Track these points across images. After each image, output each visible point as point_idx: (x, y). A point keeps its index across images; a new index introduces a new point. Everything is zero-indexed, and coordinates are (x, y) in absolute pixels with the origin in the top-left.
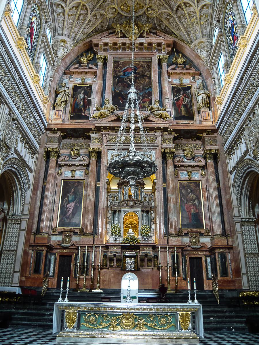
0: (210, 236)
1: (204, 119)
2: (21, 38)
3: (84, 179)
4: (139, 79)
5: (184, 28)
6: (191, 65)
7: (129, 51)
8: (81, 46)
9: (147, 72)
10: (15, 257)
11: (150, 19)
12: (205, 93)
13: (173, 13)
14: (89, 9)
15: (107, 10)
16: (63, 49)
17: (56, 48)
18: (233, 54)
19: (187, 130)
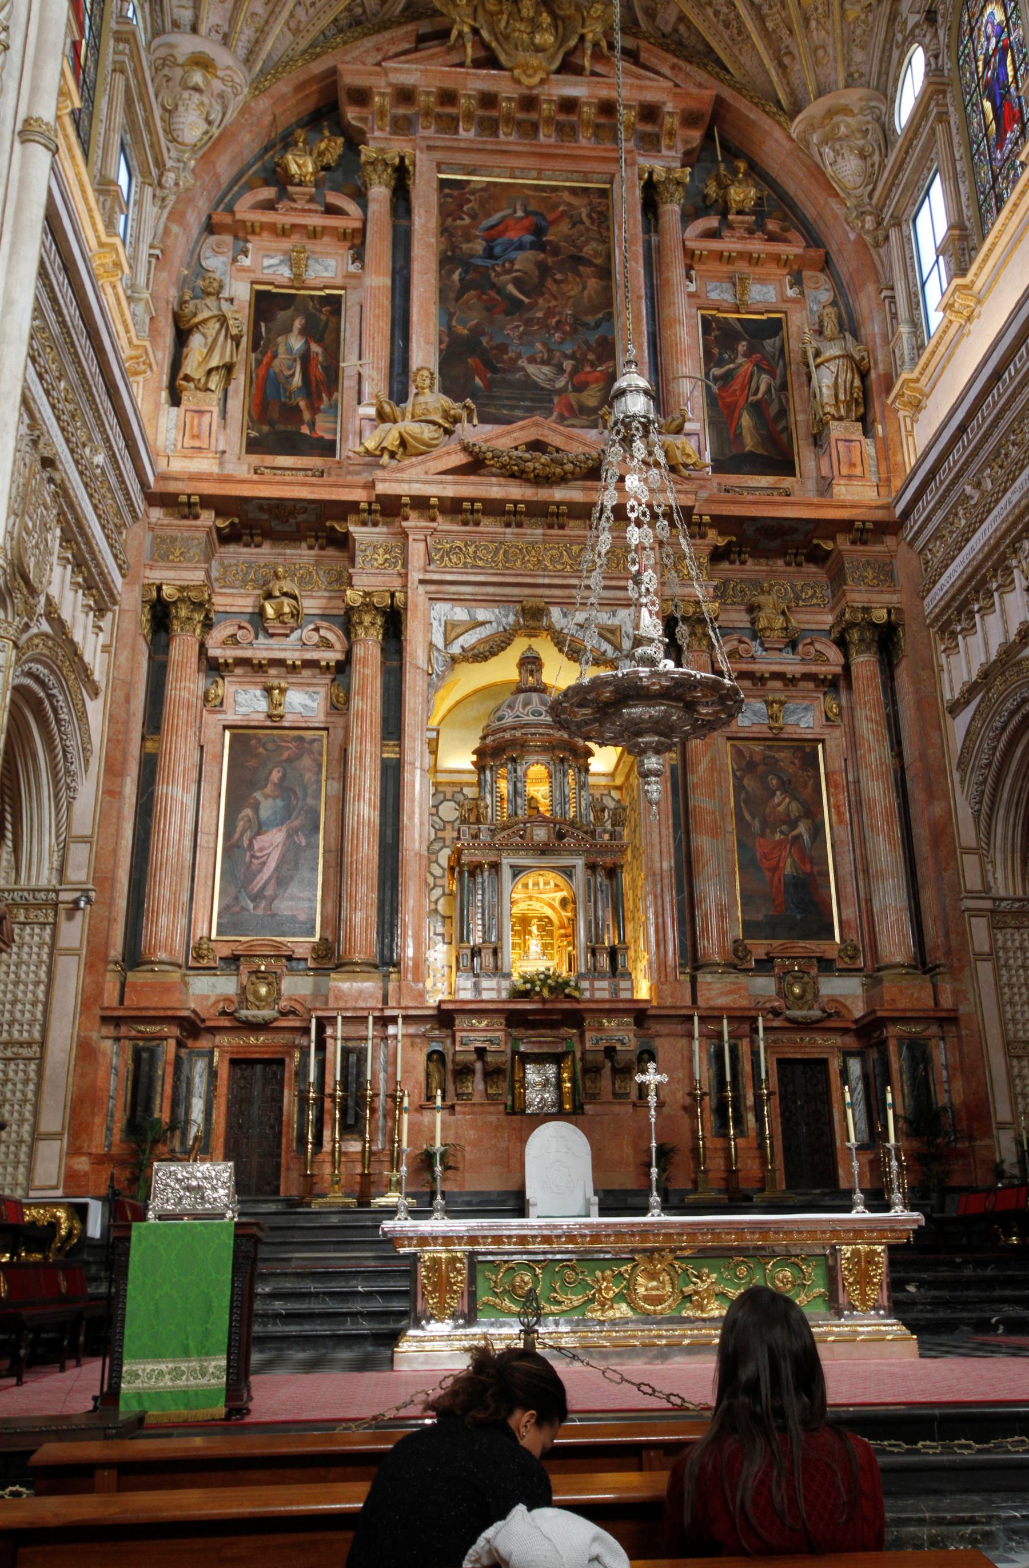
0: (860, 970)
1: (844, 471)
3: (327, 729)
4: (558, 276)
5: (766, 34)
6: (786, 215)
7: (512, 138)
8: (283, 97)
9: (594, 245)
10: (40, 1072)
12: (849, 357)
18: (993, 188)
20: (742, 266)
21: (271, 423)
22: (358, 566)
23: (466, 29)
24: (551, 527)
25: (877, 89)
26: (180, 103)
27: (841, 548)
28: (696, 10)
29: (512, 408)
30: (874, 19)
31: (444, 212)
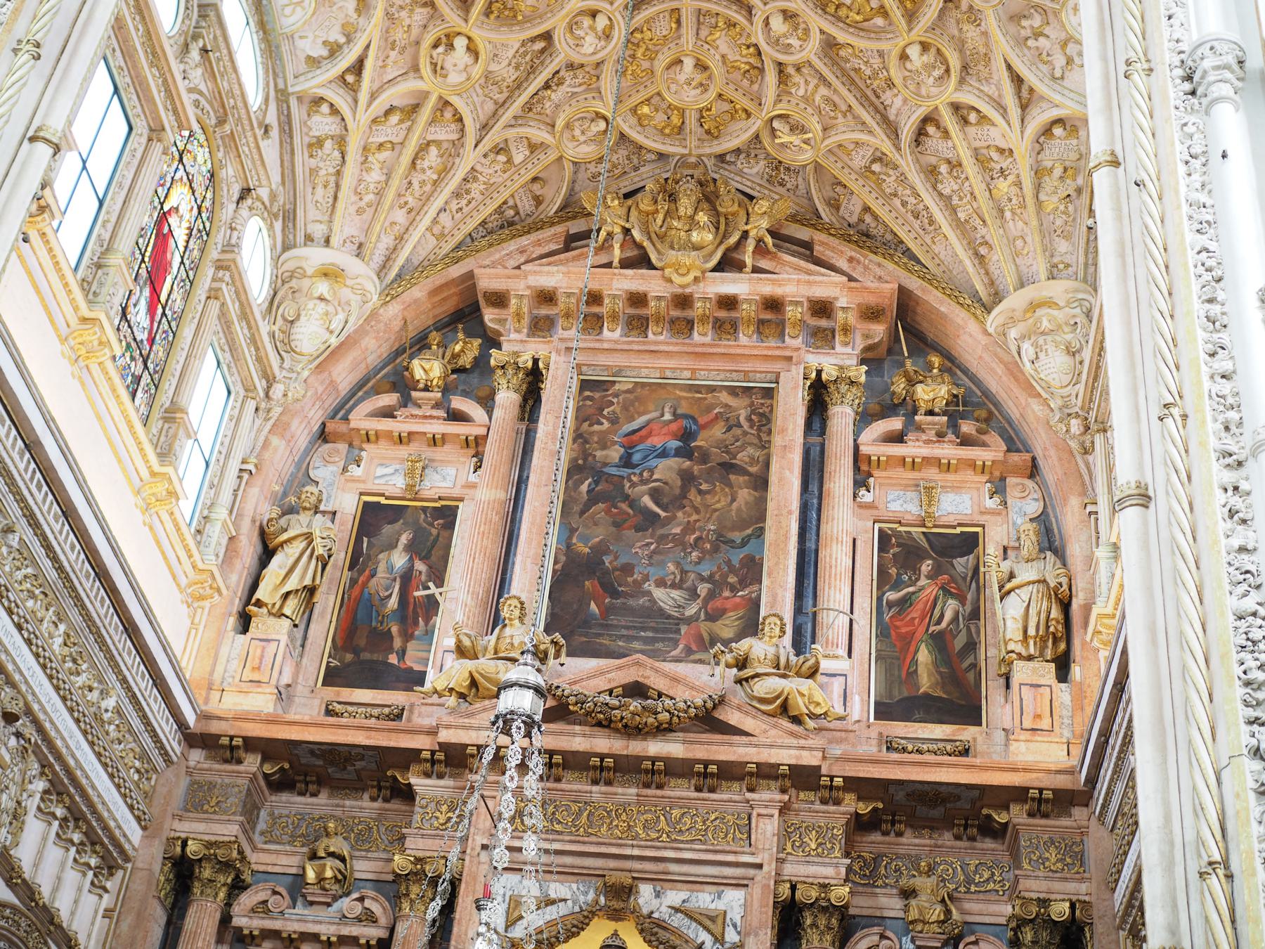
1: (1027, 724)
2: (92, 315)
4: (704, 487)
5: (960, 225)
7: (662, 338)
8: (416, 301)
9: (750, 450)
11: (788, 169)
12: (1043, 581)
13: (899, 149)
14: (468, 121)
15: (560, 123)
16: (327, 314)
17: (288, 309)
19: (920, 787)
20: (932, 473)
21: (356, 651)
22: (415, 825)
23: (617, 230)
24: (647, 785)
25: (1085, 280)
26: (303, 313)
27: (1015, 821)
28: (881, 201)
29: (629, 639)
30: (1076, 211)
31: (582, 417)
